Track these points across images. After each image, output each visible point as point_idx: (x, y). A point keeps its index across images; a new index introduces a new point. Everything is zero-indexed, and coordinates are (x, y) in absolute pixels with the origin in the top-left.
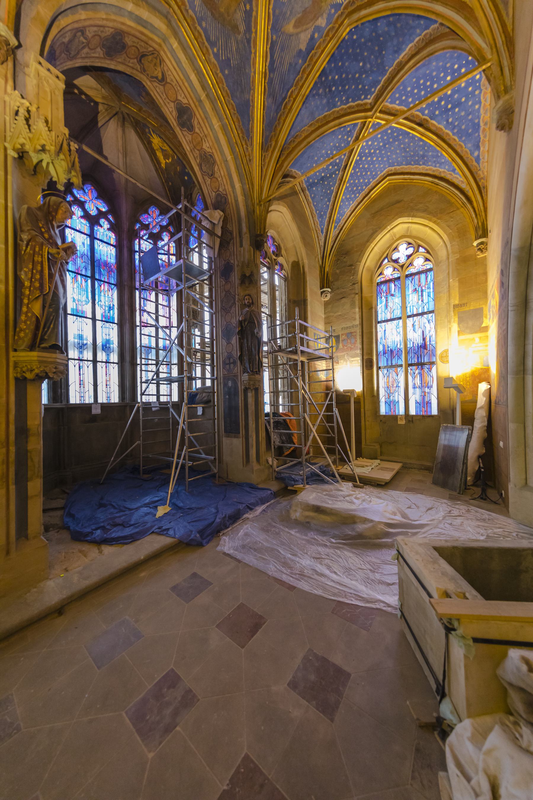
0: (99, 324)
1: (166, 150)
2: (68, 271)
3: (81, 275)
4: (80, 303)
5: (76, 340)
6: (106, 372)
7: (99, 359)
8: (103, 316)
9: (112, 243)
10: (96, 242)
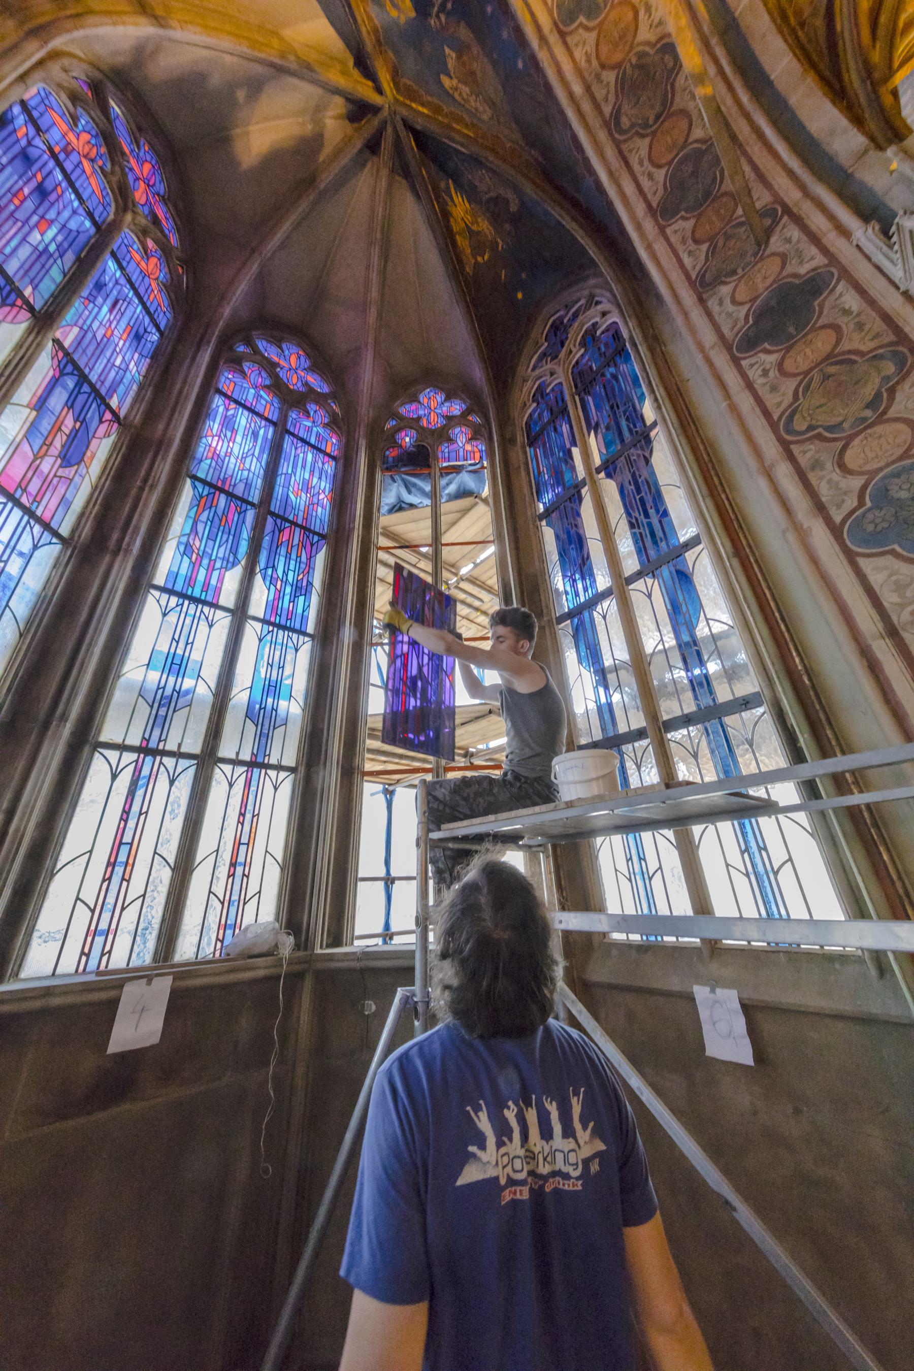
0: (252, 631)
1: (478, 233)
2: (194, 478)
3: (229, 494)
4: (205, 562)
5: (154, 676)
6: (244, 804)
7: (227, 750)
8: (273, 607)
9: (328, 451)
10: (288, 439)
